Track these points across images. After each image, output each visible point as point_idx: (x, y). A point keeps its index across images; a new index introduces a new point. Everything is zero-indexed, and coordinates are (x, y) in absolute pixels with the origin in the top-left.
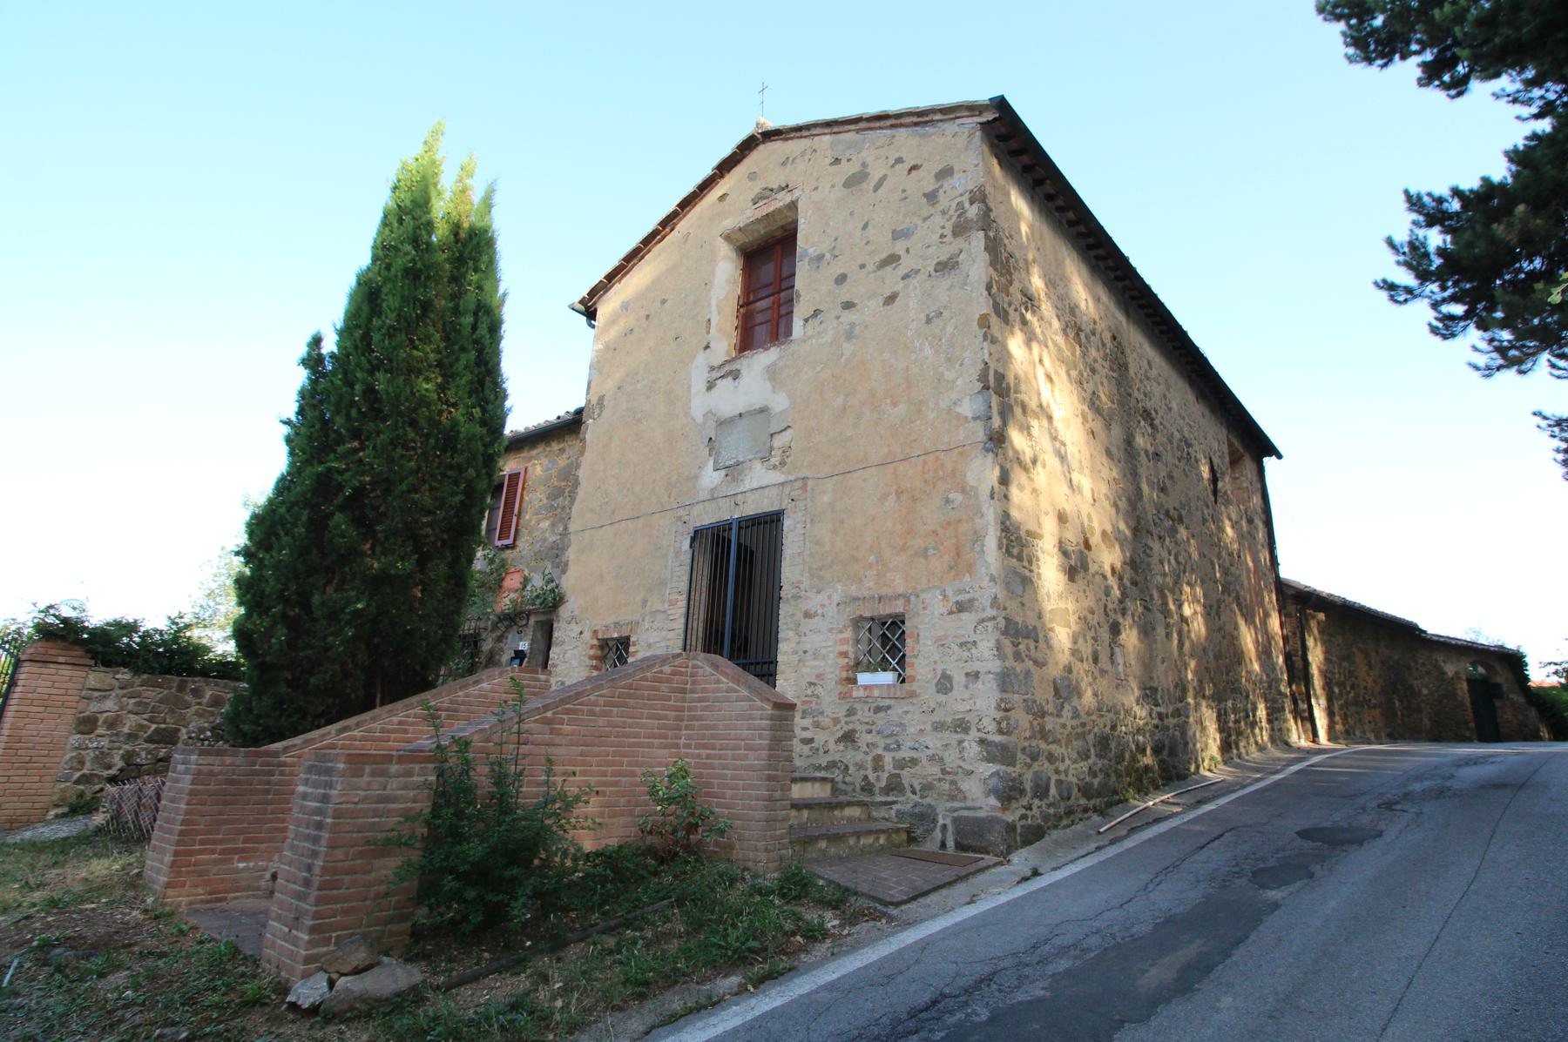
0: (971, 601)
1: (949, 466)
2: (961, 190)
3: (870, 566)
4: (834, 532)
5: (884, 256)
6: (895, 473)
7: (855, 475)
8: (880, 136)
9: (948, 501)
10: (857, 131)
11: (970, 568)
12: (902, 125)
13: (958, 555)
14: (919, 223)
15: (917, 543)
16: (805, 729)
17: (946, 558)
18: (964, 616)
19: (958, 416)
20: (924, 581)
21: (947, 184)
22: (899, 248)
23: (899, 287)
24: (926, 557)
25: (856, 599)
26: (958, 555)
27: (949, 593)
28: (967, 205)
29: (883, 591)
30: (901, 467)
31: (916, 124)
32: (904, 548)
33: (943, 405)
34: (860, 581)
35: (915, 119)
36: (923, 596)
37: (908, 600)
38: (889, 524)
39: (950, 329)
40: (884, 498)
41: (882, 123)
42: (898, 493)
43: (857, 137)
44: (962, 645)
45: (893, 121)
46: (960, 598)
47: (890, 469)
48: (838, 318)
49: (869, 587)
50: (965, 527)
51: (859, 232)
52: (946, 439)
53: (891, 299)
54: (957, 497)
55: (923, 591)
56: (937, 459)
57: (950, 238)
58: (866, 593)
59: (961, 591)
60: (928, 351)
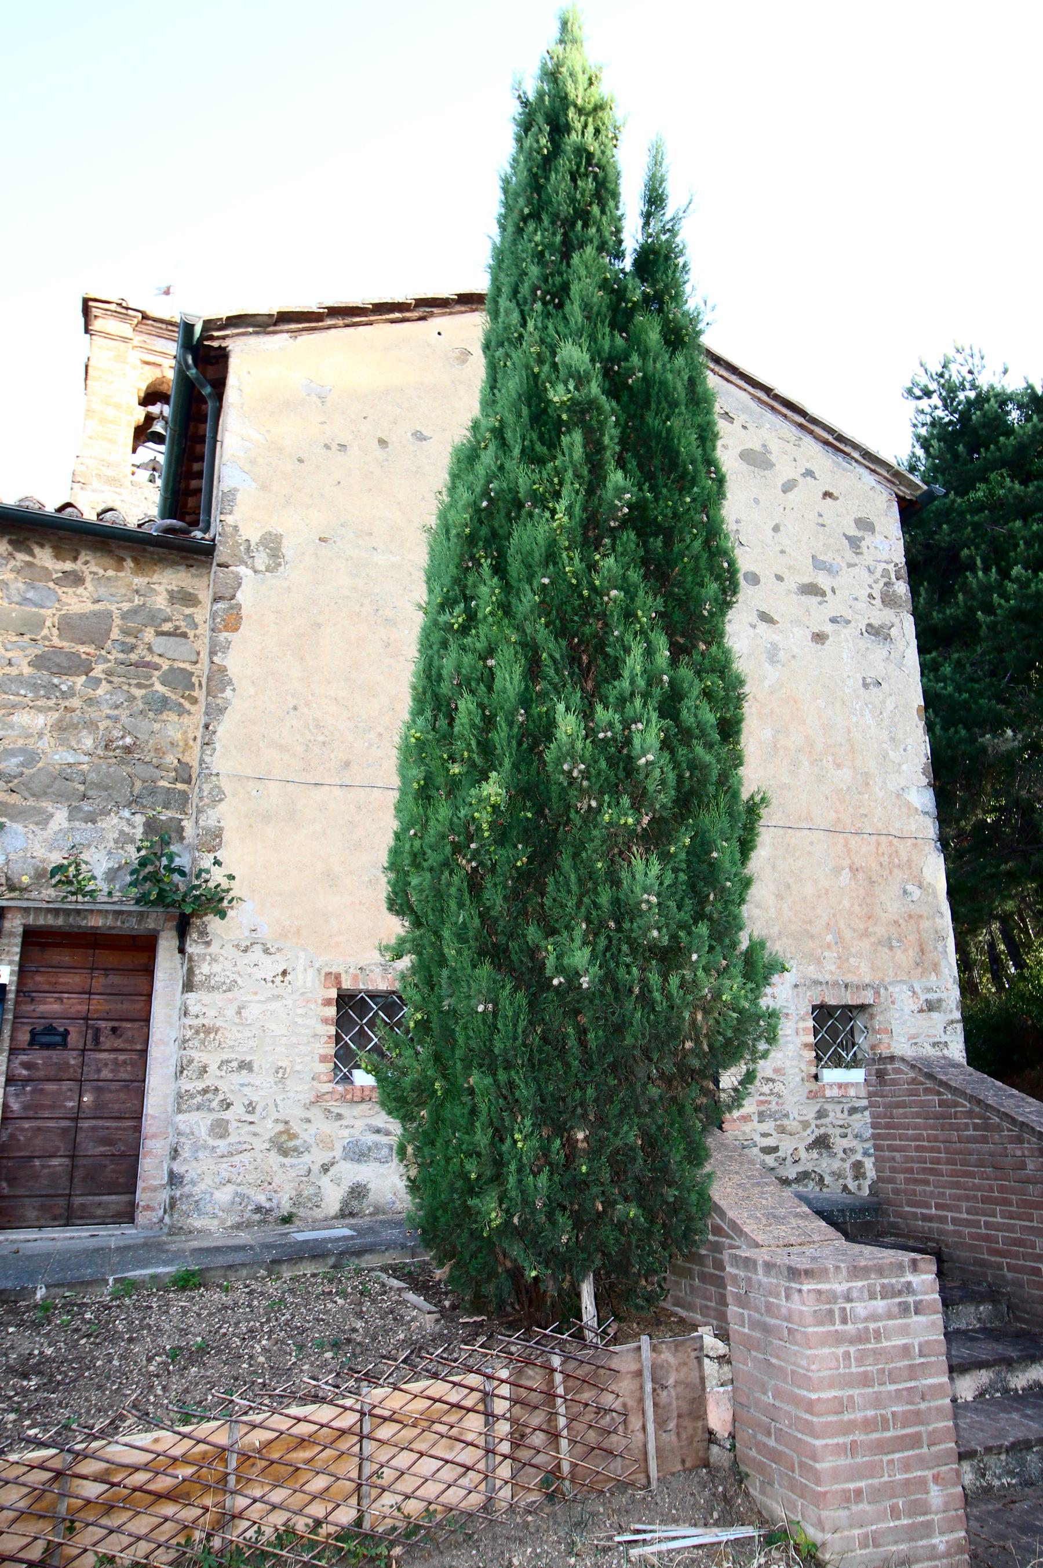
0: (940, 1000)
1: (904, 858)
2: (885, 556)
3: (829, 946)
4: (779, 897)
5: (806, 580)
6: (846, 845)
7: (799, 833)
8: (789, 431)
9: (905, 892)
10: (754, 397)
11: (935, 967)
12: (811, 432)
13: (922, 951)
14: (844, 566)
15: (881, 931)
16: (764, 1135)
17: (911, 952)
18: (934, 1015)
19: (908, 805)
20: (891, 973)
21: (869, 540)
22: (823, 581)
23: (828, 628)
24: (891, 948)
25: (817, 983)
26: (922, 951)
27: (918, 989)
28: (893, 577)
29: (850, 978)
30: (854, 841)
31: (826, 443)
32: (866, 934)
33: (892, 786)
34: (819, 962)
35: (831, 439)
36: (891, 989)
37: (877, 993)
38: (846, 903)
39: (890, 705)
40: (837, 870)
41: (789, 413)
42: (854, 870)
43: (753, 405)
44: (935, 1045)
45: (801, 420)
46: (929, 996)
47: (840, 839)
48: (754, 627)
49: (829, 970)
50: (925, 924)
51: (770, 533)
52: (897, 825)
53: (819, 638)
54: (917, 893)
55: (890, 984)
56: (891, 844)
57: (878, 602)
58: (828, 977)
59: (929, 990)
60: (869, 720)
